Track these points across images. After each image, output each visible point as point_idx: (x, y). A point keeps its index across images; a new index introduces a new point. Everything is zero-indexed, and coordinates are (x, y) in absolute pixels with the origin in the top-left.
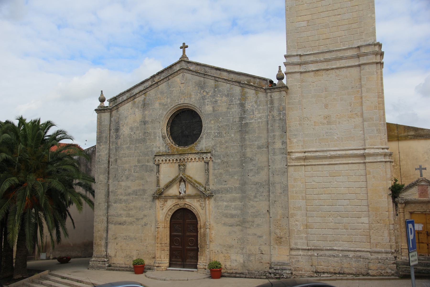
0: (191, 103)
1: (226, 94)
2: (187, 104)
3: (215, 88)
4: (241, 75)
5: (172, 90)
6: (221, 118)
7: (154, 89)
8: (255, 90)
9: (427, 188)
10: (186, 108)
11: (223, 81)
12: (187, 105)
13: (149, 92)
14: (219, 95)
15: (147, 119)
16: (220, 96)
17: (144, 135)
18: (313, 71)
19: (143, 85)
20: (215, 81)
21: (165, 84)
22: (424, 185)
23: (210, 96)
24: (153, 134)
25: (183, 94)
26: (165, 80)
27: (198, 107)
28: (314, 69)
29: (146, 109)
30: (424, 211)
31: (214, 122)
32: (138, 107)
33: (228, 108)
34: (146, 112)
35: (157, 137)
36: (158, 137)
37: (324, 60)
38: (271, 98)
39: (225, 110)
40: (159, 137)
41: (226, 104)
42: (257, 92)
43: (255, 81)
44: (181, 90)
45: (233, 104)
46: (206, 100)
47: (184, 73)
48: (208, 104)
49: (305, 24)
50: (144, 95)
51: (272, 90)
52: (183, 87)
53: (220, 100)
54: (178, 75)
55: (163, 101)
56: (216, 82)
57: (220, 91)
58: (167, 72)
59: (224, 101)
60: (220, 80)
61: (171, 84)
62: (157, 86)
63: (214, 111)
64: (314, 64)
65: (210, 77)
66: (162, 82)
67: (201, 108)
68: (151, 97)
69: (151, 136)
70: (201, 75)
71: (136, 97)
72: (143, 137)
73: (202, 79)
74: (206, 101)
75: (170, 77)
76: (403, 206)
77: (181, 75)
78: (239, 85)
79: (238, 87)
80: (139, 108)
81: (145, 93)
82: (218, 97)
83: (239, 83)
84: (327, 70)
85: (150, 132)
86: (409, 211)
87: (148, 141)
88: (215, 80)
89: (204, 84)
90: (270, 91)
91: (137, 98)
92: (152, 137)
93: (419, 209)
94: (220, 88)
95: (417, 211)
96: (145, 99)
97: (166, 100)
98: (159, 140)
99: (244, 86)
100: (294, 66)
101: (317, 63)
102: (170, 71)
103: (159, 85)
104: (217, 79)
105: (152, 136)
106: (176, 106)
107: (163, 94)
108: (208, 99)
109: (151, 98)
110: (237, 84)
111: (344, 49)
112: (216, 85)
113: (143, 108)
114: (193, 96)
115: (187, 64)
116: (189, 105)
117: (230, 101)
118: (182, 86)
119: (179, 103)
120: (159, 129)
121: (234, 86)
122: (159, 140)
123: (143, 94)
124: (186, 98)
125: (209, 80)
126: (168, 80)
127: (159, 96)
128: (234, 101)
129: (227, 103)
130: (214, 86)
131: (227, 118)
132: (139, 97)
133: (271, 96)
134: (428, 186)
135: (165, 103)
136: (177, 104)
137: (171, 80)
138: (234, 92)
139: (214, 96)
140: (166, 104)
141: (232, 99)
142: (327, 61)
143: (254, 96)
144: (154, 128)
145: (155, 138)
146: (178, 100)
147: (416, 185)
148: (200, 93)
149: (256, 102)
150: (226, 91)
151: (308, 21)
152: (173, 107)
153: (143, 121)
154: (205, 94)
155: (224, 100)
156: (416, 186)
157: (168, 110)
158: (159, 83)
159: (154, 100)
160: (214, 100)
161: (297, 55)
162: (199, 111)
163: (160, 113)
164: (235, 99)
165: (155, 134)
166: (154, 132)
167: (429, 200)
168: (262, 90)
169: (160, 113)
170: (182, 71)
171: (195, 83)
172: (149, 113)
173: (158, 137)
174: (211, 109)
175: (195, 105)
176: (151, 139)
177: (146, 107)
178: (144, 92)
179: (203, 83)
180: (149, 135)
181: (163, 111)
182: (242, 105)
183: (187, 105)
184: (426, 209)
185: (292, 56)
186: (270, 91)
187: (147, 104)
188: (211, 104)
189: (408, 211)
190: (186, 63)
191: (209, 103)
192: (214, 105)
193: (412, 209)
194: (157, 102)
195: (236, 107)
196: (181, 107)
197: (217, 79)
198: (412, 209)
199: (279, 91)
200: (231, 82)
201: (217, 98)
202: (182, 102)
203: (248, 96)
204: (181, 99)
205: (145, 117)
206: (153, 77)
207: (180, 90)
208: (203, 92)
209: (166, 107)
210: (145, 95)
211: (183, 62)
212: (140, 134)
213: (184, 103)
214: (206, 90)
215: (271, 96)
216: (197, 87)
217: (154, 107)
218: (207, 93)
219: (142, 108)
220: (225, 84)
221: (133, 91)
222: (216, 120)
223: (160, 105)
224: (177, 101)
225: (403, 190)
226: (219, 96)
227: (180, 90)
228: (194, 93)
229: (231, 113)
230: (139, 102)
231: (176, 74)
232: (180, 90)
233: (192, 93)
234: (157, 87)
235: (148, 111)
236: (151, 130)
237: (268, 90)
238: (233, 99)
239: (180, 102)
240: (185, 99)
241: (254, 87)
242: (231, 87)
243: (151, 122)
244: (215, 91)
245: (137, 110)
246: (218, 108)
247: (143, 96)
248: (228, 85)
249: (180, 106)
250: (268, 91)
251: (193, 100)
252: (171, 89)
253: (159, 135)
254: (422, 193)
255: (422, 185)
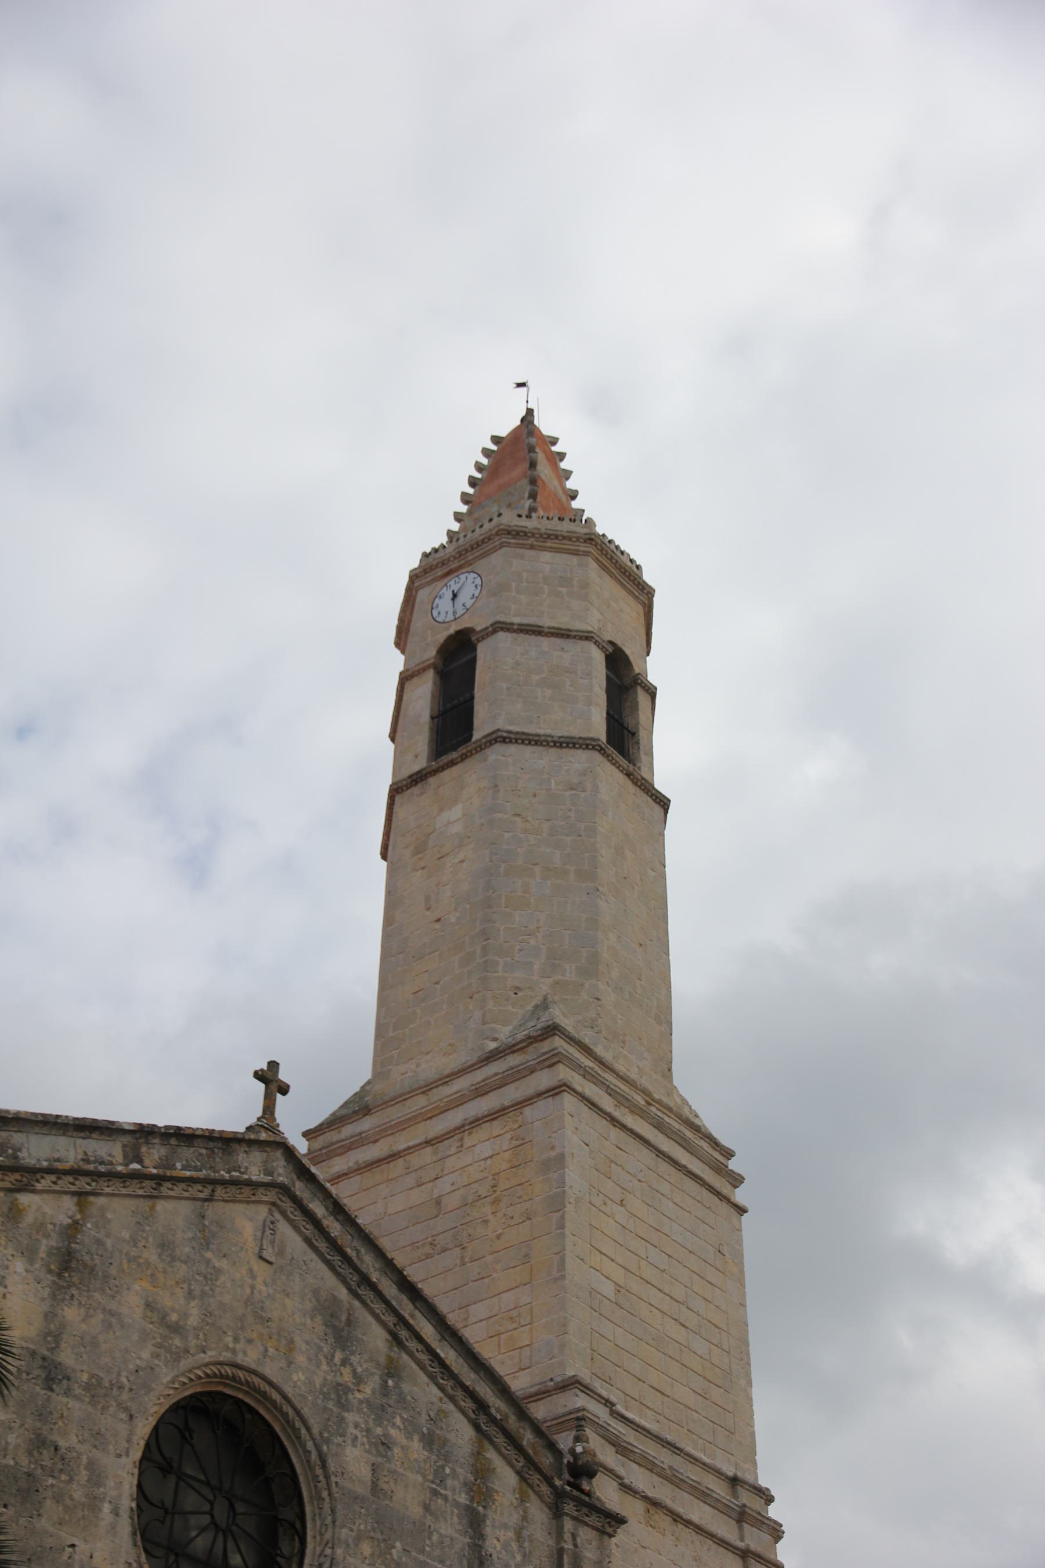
0: (289, 1391)
1: (425, 1430)
2: (271, 1384)
3: (390, 1375)
4: (482, 1374)
5: (217, 1265)
6: (398, 1544)
7: (132, 1203)
8: (518, 1473)
10: (247, 1400)
11: (424, 1357)
12: (267, 1388)
13: (101, 1201)
14: (402, 1417)
15: (66, 1357)
16: (402, 1427)
17: (30, 1454)
18: (646, 1498)
19: (79, 1141)
20: (390, 1338)
21: (185, 1208)
23: (368, 1401)
24: (84, 1475)
25: (261, 1317)
26: (195, 1190)
27: (315, 1431)
28: (650, 1494)
29: (74, 1291)
31: (372, 1555)
32: (29, 1253)
33: (427, 1508)
34: (71, 1313)
35: (102, 1500)
36: (106, 1508)
37: (668, 1472)
38: (575, 1545)
39: (415, 1511)
40: (116, 1512)
41: (420, 1478)
42: (524, 1485)
43: (521, 1430)
44: (252, 1293)
45: (445, 1498)
46: (348, 1410)
47: (277, 1215)
48: (356, 1437)
49: (608, 1289)
50: (75, 1199)
51: (585, 1510)
52: (266, 1285)
53: (403, 1448)
54: (248, 1202)
55: (166, 1301)
56: (391, 1348)
57: (402, 1399)
58: (204, 1151)
59: (416, 1460)
60: (413, 1345)
61: (214, 1228)
62: (151, 1197)
63: (375, 1486)
64: (642, 1470)
65: (378, 1307)
66: (178, 1190)
67: (328, 1441)
68: (108, 1235)
69: (71, 1480)
70: (346, 1271)
71: (39, 1186)
72: (24, 1461)
73: (343, 1293)
74: (351, 1417)
75: (220, 1191)
77: (263, 1211)
78: (473, 1416)
79: (465, 1420)
80: (31, 1261)
81: (80, 1194)
82: (394, 1425)
83: (482, 1406)
84: (677, 1518)
85: (69, 1449)
87: (48, 1502)
88: (391, 1333)
89: (349, 1322)
90: (575, 1513)
91: (34, 1191)
92: (78, 1494)
94: (406, 1387)
96: (75, 1227)
97: (182, 1301)
98: (113, 1528)
99: (492, 1430)
100: (603, 1441)
101: (651, 1471)
102: (218, 1160)
103: (157, 1197)
104: (403, 1334)
105: (74, 1486)
106: (221, 1364)
107: (173, 1258)
108: (359, 1410)
109: (109, 1243)
110: (468, 1405)
111: (704, 1464)
112: (391, 1360)
113: (60, 1275)
114: (301, 1359)
115: (295, 1177)
116: (276, 1396)
117: (436, 1472)
118: (259, 1267)
119: (240, 1359)
120: (124, 1460)
121: (452, 1407)
122: (113, 1528)
123: (74, 1194)
124: (271, 1350)
125: (370, 1318)
126: (206, 1200)
127: (151, 1255)
128: (449, 1482)
129: (424, 1476)
130: (382, 1360)
131: (421, 1557)
132: (46, 1196)
133: (574, 1536)
135: (174, 1317)
136: (226, 1356)
137: (216, 1204)
138: (451, 1436)
139: (380, 1412)
140: (177, 1323)
141: (443, 1467)
142: (674, 1480)
143: (515, 1502)
144: (98, 1438)
145: (93, 1503)
146: (236, 1339)
148: (330, 1359)
149: (519, 1537)
150: (424, 1417)
151: (618, 1287)
152: (207, 1365)
153: (44, 1359)
154: (347, 1377)
155: (416, 1456)
157: (185, 1364)
158: (165, 1189)
159: (125, 1266)
160: (379, 1431)
161: (607, 1401)
162: (314, 1456)
163: (140, 1358)
164: (454, 1475)
165: (97, 1477)
166: (91, 1465)
168: (545, 1489)
169: (140, 1358)
170: (271, 1196)
171: (316, 1292)
172: (84, 1326)
173: (106, 1508)
174: (366, 1473)
175: (306, 1411)
176: (68, 1502)
177: (75, 1279)
178: (82, 1184)
179: (344, 1318)
180: (61, 1471)
181: (158, 1356)
182: (475, 1523)
183: (267, 1388)
185: (596, 1393)
186: (575, 1513)
187: (85, 1265)
188: (367, 1447)
190: (291, 1167)
191: (359, 1434)
192: (379, 1460)
194: (137, 1287)
195: (455, 1519)
196: (226, 1385)
197: (403, 1334)
199: (597, 1529)
200: (451, 1383)
201: (392, 1432)
202: (250, 1357)
203: (497, 1492)
204: (250, 1341)
205: (57, 1338)
206: (145, 1132)
207: (248, 1291)
208: (344, 1362)
209: (177, 1342)
210: (82, 1207)
211: (279, 1153)
212: (12, 1439)
213: (260, 1369)
214: (353, 1358)
215: (574, 1536)
216: (319, 1319)
217: (113, 1306)
218: (359, 1380)
219: (50, 1271)
220: (423, 1378)
221: (18, 1138)
222: (378, 1540)
223: (149, 1314)
224: (229, 1340)
226: (398, 1421)
227: (252, 1288)
228: (307, 1343)
229: (435, 1537)
230: (40, 1227)
231: (247, 1190)
232: (252, 1288)
233: (298, 1340)
234: (149, 1203)
235: (83, 1310)
236: (75, 1439)
237: (572, 1504)
238: (448, 1471)
239: (245, 1353)
240: (266, 1350)
241: (522, 1459)
242: (444, 1406)
243: (88, 1387)
244: (385, 1390)
245: (19, 1266)
246: (392, 1483)
247: (69, 1204)
248: (435, 1390)
249: (234, 1378)
250: (569, 1508)
251: (298, 1377)
252: (209, 1255)
253: (114, 1493)
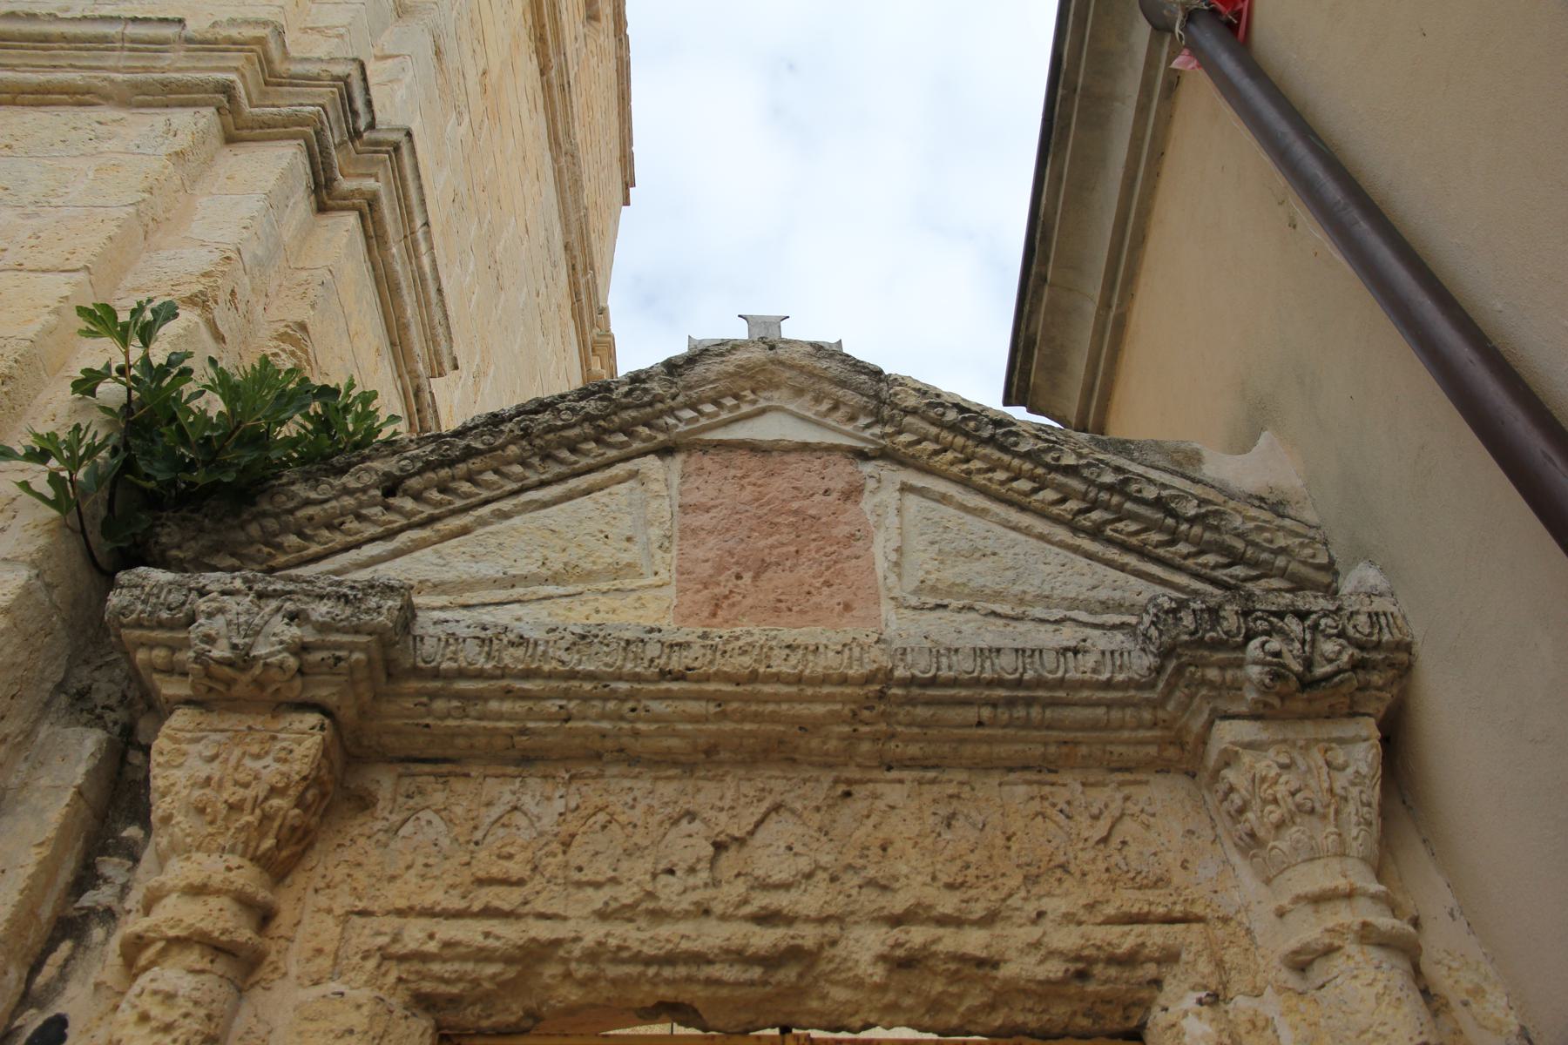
9: (853, 493)
22: (804, 447)
30: (765, 939)
76: (270, 770)
86: (415, 934)
93: (670, 892)
95: (593, 933)
134: (868, 468)
147: (665, 451)
156: (651, 464)
167: (877, 658)
184: (808, 901)
189: (366, 935)
193: (487, 896)
198: (487, 896)
225: (392, 486)
254: (762, 567)
255: (753, 448)
